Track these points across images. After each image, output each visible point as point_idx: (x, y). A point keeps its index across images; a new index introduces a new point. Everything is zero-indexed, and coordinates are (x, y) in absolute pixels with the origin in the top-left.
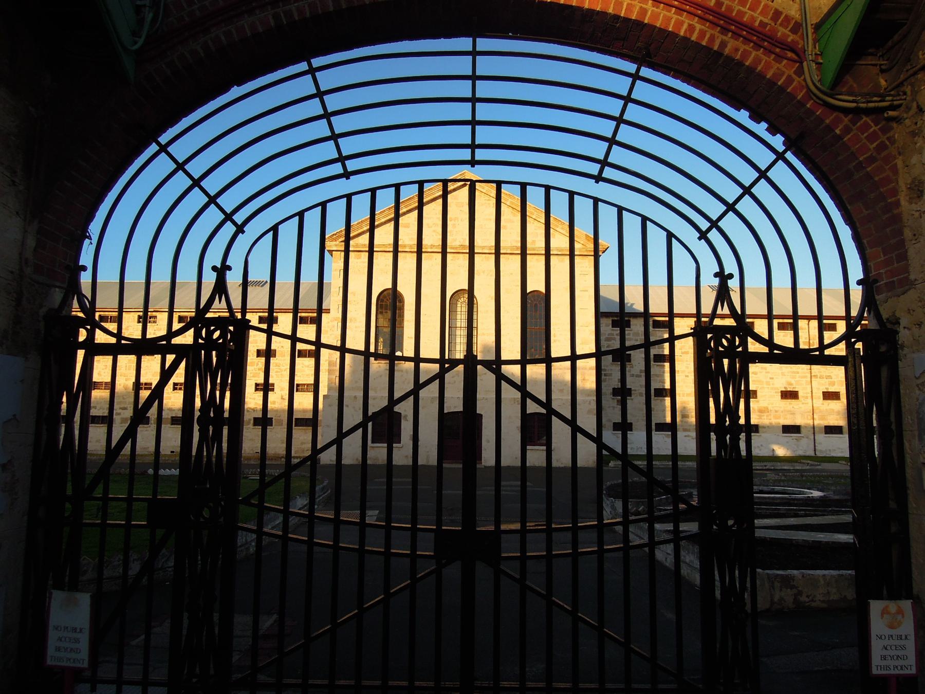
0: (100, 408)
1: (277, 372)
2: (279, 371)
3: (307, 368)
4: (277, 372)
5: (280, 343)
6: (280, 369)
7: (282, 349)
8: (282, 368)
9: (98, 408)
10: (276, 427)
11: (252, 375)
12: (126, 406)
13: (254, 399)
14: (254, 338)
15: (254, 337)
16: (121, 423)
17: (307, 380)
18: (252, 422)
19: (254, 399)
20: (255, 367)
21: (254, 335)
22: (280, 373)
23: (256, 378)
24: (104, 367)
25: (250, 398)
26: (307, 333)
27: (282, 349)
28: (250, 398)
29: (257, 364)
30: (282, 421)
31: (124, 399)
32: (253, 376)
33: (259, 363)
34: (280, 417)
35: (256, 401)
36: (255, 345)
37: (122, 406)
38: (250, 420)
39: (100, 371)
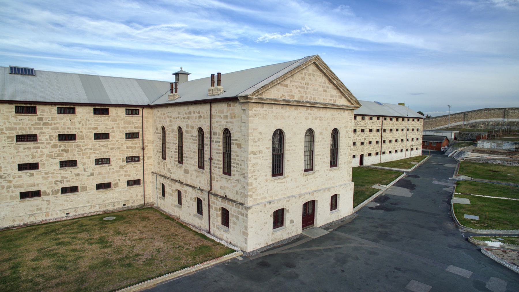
1: (78, 151)
2: (79, 150)
3: (102, 147)
5: (79, 129)
6: (81, 149)
7: (81, 134)
8: (82, 148)
10: (81, 192)
11: (56, 155)
13: (61, 174)
14: (55, 126)
15: (55, 125)
17: (104, 156)
18: (60, 191)
19: (61, 174)
20: (58, 148)
21: (55, 123)
22: (81, 152)
23: (61, 158)
25: (56, 174)
26: (101, 121)
27: (81, 134)
28: (56, 174)
29: (60, 147)
30: (87, 187)
32: (57, 156)
33: (62, 145)
34: (84, 184)
35: (62, 175)
36: (56, 131)
38: (58, 190)
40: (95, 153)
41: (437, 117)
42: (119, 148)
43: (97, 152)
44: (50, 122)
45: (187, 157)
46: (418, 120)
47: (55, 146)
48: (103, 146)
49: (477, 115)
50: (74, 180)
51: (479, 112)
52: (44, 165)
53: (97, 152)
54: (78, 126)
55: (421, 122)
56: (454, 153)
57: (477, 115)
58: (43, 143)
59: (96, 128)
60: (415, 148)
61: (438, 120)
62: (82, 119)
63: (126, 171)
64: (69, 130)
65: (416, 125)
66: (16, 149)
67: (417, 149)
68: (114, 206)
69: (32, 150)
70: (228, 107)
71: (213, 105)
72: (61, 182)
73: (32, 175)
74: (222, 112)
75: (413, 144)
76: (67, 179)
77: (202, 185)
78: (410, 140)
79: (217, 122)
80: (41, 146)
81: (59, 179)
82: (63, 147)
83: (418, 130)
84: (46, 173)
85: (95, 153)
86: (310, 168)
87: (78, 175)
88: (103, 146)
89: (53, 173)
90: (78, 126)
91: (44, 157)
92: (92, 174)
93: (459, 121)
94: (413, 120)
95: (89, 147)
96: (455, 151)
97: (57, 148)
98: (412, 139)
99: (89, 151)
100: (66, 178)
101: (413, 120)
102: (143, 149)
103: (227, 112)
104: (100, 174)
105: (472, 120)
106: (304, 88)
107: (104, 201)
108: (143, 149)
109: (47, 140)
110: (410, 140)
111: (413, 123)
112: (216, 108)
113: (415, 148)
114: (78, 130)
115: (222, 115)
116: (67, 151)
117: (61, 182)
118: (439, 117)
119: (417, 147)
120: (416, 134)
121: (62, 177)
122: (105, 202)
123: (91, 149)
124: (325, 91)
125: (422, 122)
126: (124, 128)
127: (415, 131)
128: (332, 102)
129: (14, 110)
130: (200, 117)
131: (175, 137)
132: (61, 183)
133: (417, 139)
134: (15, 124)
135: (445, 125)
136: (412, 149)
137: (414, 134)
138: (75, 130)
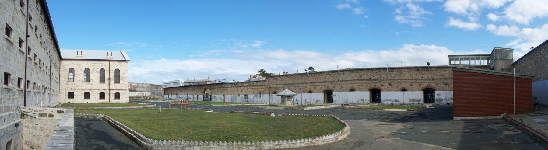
79: (113, 67)
112: (111, 63)
115: (115, 65)
130: (103, 65)
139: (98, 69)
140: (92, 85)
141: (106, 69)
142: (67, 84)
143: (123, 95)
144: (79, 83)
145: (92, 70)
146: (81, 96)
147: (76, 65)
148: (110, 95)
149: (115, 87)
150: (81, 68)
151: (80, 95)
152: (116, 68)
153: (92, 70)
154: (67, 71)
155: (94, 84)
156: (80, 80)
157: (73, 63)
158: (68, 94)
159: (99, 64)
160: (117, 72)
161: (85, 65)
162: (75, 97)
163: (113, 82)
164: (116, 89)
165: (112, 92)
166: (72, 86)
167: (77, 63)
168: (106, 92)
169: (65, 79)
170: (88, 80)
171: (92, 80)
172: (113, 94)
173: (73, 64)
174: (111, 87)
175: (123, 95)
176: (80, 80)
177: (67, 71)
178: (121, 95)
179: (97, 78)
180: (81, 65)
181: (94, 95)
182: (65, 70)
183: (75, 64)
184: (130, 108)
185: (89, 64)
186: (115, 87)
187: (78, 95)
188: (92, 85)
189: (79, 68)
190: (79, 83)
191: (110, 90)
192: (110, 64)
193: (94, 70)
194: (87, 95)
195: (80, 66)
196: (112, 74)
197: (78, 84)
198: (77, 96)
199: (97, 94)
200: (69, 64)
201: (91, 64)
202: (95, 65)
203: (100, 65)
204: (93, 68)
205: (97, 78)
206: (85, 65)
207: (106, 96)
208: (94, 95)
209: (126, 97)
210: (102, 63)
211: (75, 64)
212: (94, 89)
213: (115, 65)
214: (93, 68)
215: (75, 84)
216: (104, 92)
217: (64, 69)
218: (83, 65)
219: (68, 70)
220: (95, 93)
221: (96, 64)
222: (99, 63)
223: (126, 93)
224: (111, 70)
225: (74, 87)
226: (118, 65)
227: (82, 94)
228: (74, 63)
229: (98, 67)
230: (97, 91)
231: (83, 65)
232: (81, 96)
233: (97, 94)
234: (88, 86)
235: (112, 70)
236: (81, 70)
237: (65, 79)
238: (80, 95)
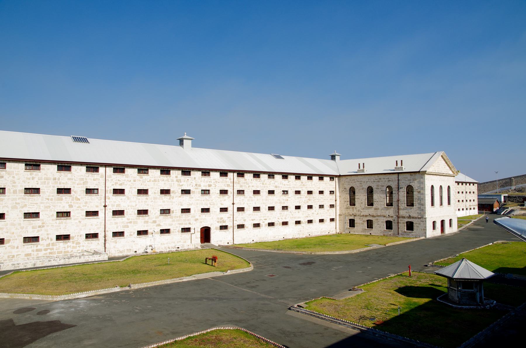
0: (257, 220)
1: (313, 200)
4: (313, 200)
9: (256, 220)
11: (306, 202)
12: (266, 218)
13: (307, 212)
16: (265, 226)
19: (307, 212)
24: (257, 200)
31: (265, 215)
32: (307, 203)
35: (308, 213)
36: (307, 189)
37: (265, 218)
39: (255, 202)
40: (319, 202)
41: (484, 183)
42: (327, 199)
43: (320, 201)
44: (305, 184)
45: (377, 202)
46: (473, 185)
47: (306, 197)
48: (322, 198)
49: (522, 180)
50: (312, 216)
51: (524, 177)
52: (302, 207)
53: (320, 201)
54: (314, 186)
55: (475, 186)
56: (505, 212)
57: (522, 180)
58: (302, 195)
59: (319, 188)
60: (472, 208)
61: (486, 185)
62: (315, 183)
63: (330, 213)
64: (311, 189)
65: (472, 188)
66: (295, 198)
67: (474, 209)
68: (325, 233)
69: (300, 199)
70: (411, 175)
71: (399, 175)
72: (308, 217)
73: (299, 212)
74: (407, 178)
75: (471, 205)
76: (310, 215)
77: (390, 214)
78: (468, 201)
79: (403, 183)
80: (302, 197)
81: (307, 215)
82: (309, 198)
83: (474, 192)
84: (303, 212)
85: (319, 202)
86: (441, 204)
87: (313, 213)
88: (322, 198)
89: (305, 212)
90: (314, 186)
91: (303, 202)
92: (318, 214)
93: (506, 186)
94: (470, 185)
95: (317, 198)
96: (506, 210)
97: (306, 198)
98: (470, 201)
99: (317, 200)
100: (309, 215)
101: (470, 185)
102: (336, 201)
103: (410, 178)
104: (320, 213)
105: (518, 184)
106: (438, 166)
107: (321, 229)
108: (336, 201)
109: (304, 194)
110: (468, 201)
111: (470, 186)
112: (401, 176)
113: (472, 208)
114: (313, 189)
115: (406, 179)
116: (309, 200)
117: (308, 217)
118: (487, 183)
119: (474, 207)
120: (472, 196)
121: (308, 214)
122: (322, 230)
123: (318, 199)
124: (445, 167)
125: (477, 186)
126: (329, 188)
127: (472, 193)
128: (447, 173)
129: (295, 178)
130: (389, 181)
131: (365, 192)
132: (308, 217)
133: (474, 200)
134: (295, 185)
135: (493, 190)
136: (470, 209)
137: (471, 196)
138: (312, 189)
139: (383, 186)
140: (376, 209)
141: (394, 185)
142: (348, 208)
143: (417, 225)
144: (361, 206)
145: (376, 188)
146: (363, 224)
147: (357, 183)
148: (400, 224)
149: (407, 212)
150: (362, 186)
151: (362, 224)
152: (408, 183)
153: (376, 188)
154: (346, 191)
155: (378, 209)
156: (362, 203)
157: (353, 180)
158: (348, 221)
159: (384, 180)
160: (410, 190)
161: (367, 182)
162: (355, 225)
163: (403, 204)
164: (408, 215)
165: (402, 220)
166: (353, 211)
167: (358, 180)
168: (394, 220)
169: (345, 201)
170: (370, 203)
171: (376, 203)
172: (403, 223)
173: (353, 182)
174: (402, 213)
175: (417, 225)
176: (362, 203)
177: (346, 191)
178: (414, 225)
179: (382, 200)
180: (362, 183)
181: (378, 224)
182: (345, 190)
183: (356, 181)
184: (102, 288)
185: (372, 181)
186: (407, 212)
187: (359, 223)
188: (376, 209)
189: (360, 186)
190: (361, 206)
191: (398, 217)
192: (399, 179)
193: (378, 189)
194: (370, 224)
195: (361, 184)
196: (402, 193)
197: (360, 207)
198: (358, 224)
199: (382, 222)
200: (349, 182)
201: (375, 180)
202: (379, 181)
203: (385, 181)
204: (377, 186)
205: (382, 200)
206: (367, 182)
207: (394, 226)
208: (378, 224)
209: (423, 229)
210: (388, 178)
211: (356, 181)
212: (379, 215)
213: (406, 179)
214: (377, 186)
215: (356, 208)
216: (391, 220)
217: (343, 189)
218: (364, 182)
219: (349, 190)
220: (379, 221)
221: (380, 180)
222: (384, 179)
223: (421, 222)
224: (401, 188)
225: (355, 212)
226: (410, 180)
227: (364, 221)
228: (354, 180)
229: (383, 184)
230: (382, 218)
231: (364, 182)
232: (363, 224)
233: (382, 222)
234: (371, 211)
235: (402, 188)
236: (363, 189)
237: (345, 201)
238: (362, 224)
